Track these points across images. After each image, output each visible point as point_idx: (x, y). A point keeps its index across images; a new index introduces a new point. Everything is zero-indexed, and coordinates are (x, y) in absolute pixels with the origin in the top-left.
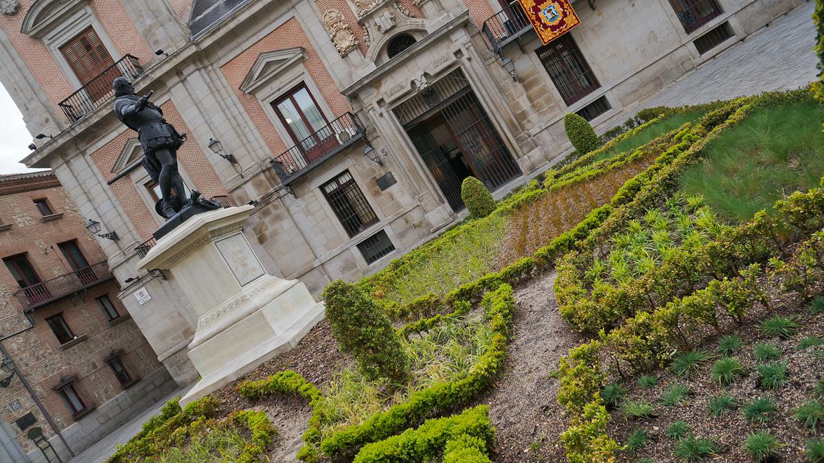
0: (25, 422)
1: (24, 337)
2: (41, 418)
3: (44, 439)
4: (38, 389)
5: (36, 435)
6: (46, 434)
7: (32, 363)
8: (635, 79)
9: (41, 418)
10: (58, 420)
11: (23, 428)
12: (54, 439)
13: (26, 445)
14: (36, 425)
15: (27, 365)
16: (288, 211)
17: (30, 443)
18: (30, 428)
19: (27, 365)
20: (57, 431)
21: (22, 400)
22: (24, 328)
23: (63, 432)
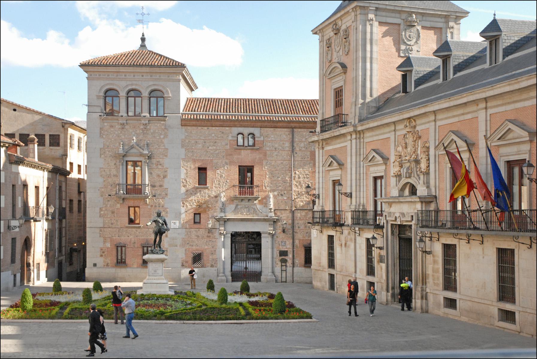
0: (283, 253)
1: (306, 213)
2: (290, 255)
3: (286, 266)
4: (297, 242)
5: (284, 261)
6: (288, 264)
7: (302, 227)
8: (470, 303)
9: (290, 255)
10: (297, 261)
11: (280, 255)
12: (289, 269)
13: (277, 264)
14: (286, 258)
15: (299, 227)
16: (355, 239)
17: (279, 264)
18: (283, 257)
19: (299, 227)
20: (293, 267)
21: (287, 243)
22: (309, 208)
23: (296, 269)
